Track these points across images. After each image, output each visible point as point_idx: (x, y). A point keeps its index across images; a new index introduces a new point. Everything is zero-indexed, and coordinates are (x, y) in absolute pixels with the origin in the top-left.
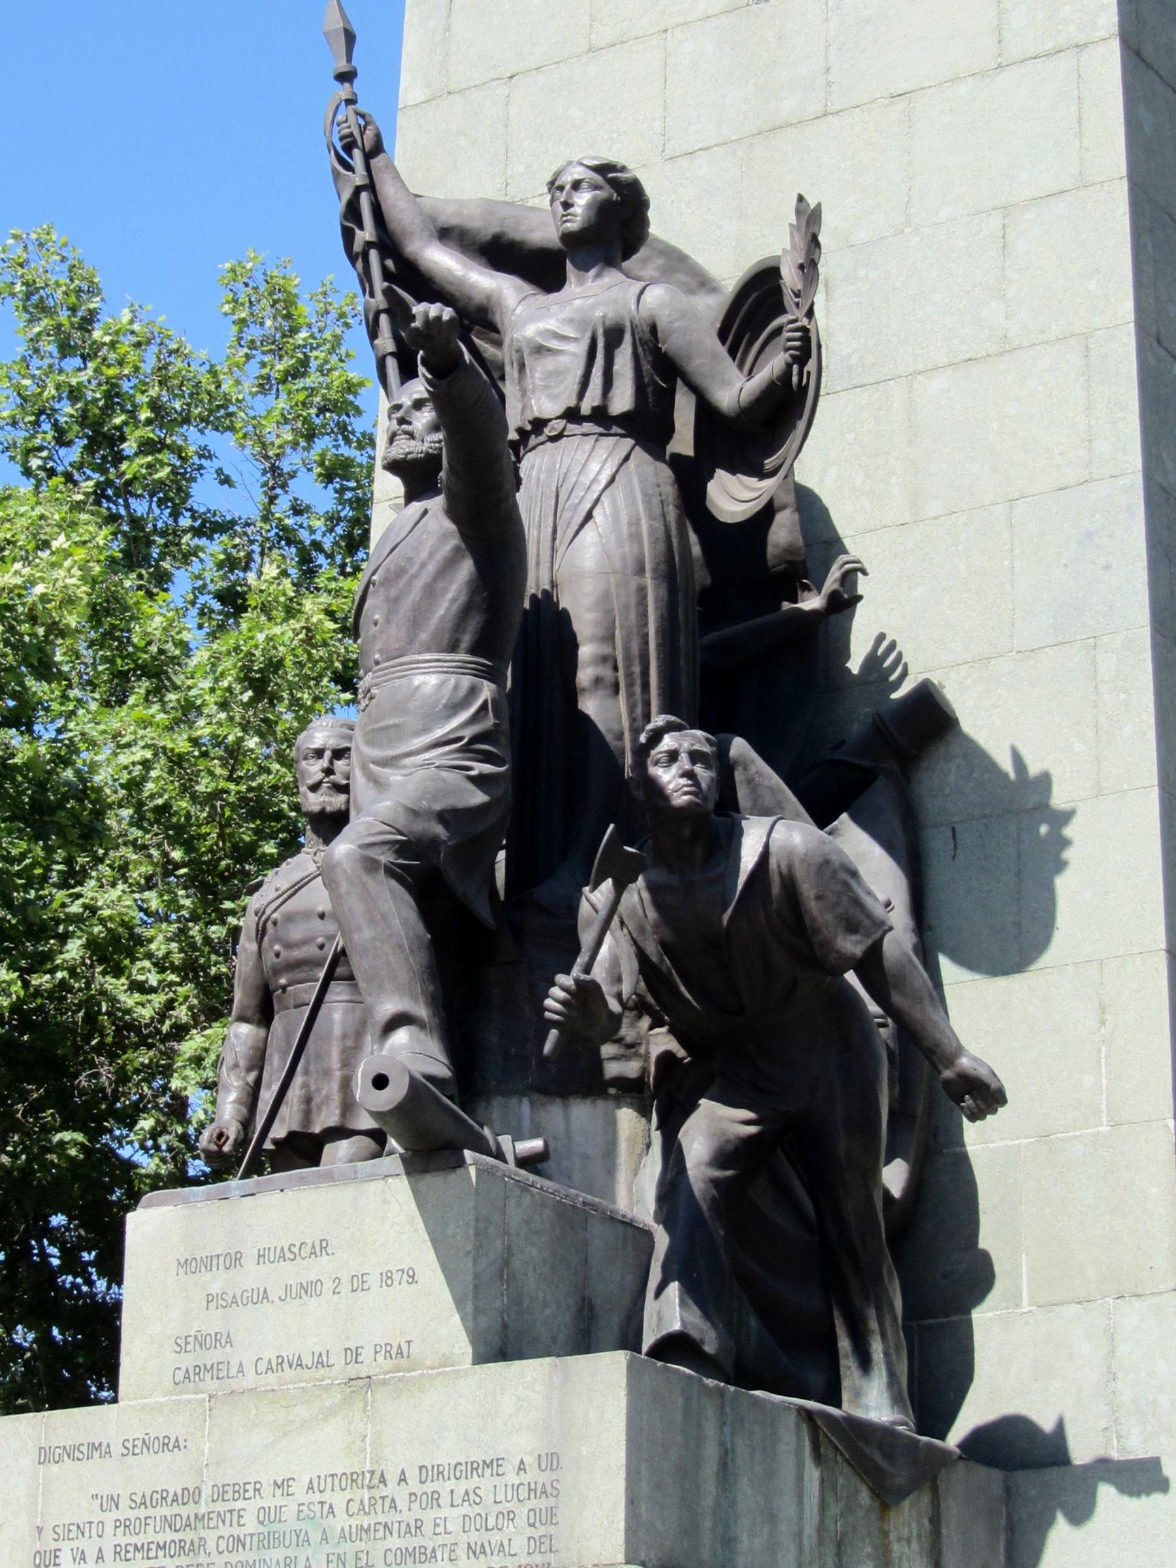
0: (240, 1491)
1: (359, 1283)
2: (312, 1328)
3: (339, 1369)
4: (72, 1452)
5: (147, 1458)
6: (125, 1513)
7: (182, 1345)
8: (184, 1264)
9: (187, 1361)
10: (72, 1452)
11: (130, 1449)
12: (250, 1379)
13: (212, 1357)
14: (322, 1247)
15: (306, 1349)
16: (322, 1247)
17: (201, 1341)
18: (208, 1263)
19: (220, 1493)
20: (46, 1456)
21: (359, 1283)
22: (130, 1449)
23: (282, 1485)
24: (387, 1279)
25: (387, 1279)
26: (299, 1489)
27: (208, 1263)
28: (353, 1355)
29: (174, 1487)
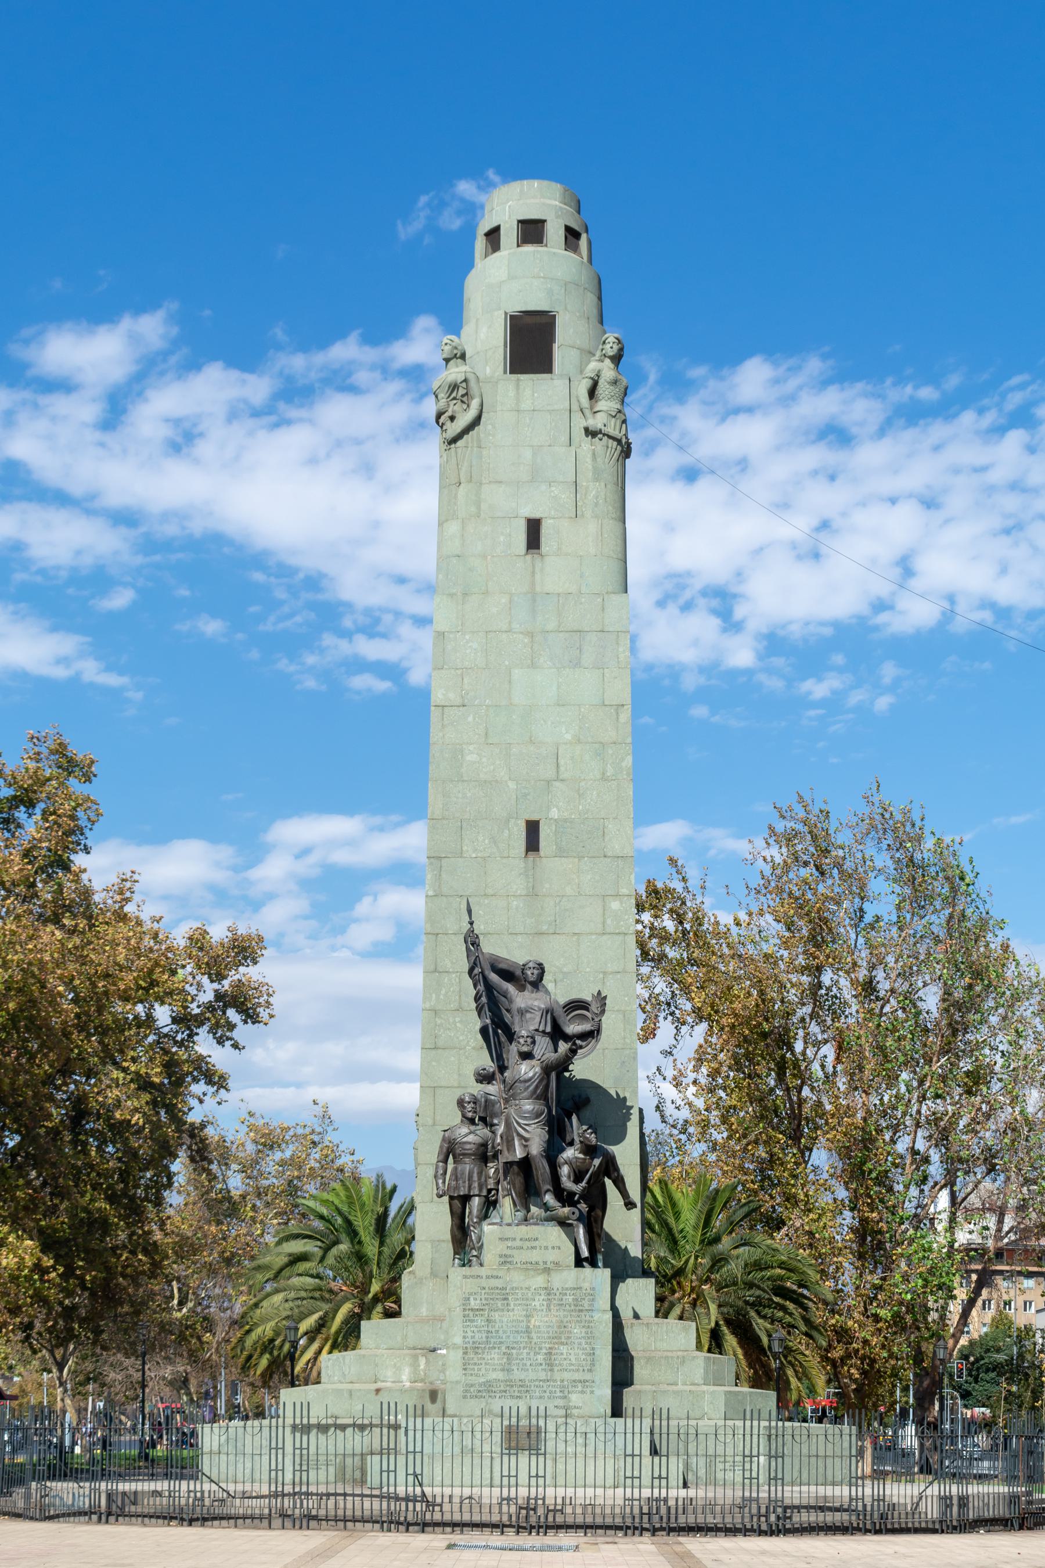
0: (517, 1288)
1: (546, 1248)
2: (535, 1256)
3: (541, 1266)
4: (472, 1277)
5: (492, 1280)
6: (487, 1290)
7: (501, 1256)
8: (500, 1239)
9: (502, 1260)
10: (472, 1277)
11: (488, 1277)
12: (519, 1265)
13: (509, 1260)
14: (537, 1239)
15: (533, 1260)
16: (537, 1239)
17: (506, 1256)
18: (507, 1239)
19: (512, 1289)
20: (465, 1277)
21: (546, 1248)
22: (488, 1277)
23: (528, 1289)
24: (553, 1248)
25: (553, 1248)
26: (532, 1290)
27: (507, 1239)
28: (545, 1263)
29: (500, 1286)
